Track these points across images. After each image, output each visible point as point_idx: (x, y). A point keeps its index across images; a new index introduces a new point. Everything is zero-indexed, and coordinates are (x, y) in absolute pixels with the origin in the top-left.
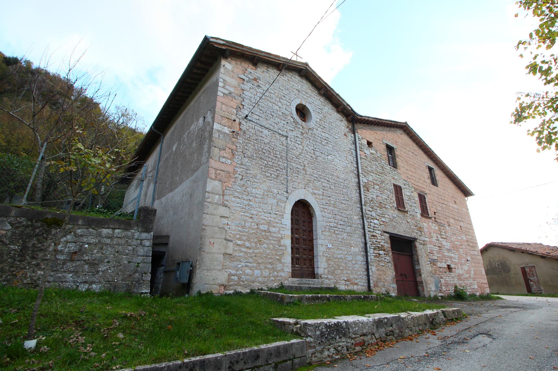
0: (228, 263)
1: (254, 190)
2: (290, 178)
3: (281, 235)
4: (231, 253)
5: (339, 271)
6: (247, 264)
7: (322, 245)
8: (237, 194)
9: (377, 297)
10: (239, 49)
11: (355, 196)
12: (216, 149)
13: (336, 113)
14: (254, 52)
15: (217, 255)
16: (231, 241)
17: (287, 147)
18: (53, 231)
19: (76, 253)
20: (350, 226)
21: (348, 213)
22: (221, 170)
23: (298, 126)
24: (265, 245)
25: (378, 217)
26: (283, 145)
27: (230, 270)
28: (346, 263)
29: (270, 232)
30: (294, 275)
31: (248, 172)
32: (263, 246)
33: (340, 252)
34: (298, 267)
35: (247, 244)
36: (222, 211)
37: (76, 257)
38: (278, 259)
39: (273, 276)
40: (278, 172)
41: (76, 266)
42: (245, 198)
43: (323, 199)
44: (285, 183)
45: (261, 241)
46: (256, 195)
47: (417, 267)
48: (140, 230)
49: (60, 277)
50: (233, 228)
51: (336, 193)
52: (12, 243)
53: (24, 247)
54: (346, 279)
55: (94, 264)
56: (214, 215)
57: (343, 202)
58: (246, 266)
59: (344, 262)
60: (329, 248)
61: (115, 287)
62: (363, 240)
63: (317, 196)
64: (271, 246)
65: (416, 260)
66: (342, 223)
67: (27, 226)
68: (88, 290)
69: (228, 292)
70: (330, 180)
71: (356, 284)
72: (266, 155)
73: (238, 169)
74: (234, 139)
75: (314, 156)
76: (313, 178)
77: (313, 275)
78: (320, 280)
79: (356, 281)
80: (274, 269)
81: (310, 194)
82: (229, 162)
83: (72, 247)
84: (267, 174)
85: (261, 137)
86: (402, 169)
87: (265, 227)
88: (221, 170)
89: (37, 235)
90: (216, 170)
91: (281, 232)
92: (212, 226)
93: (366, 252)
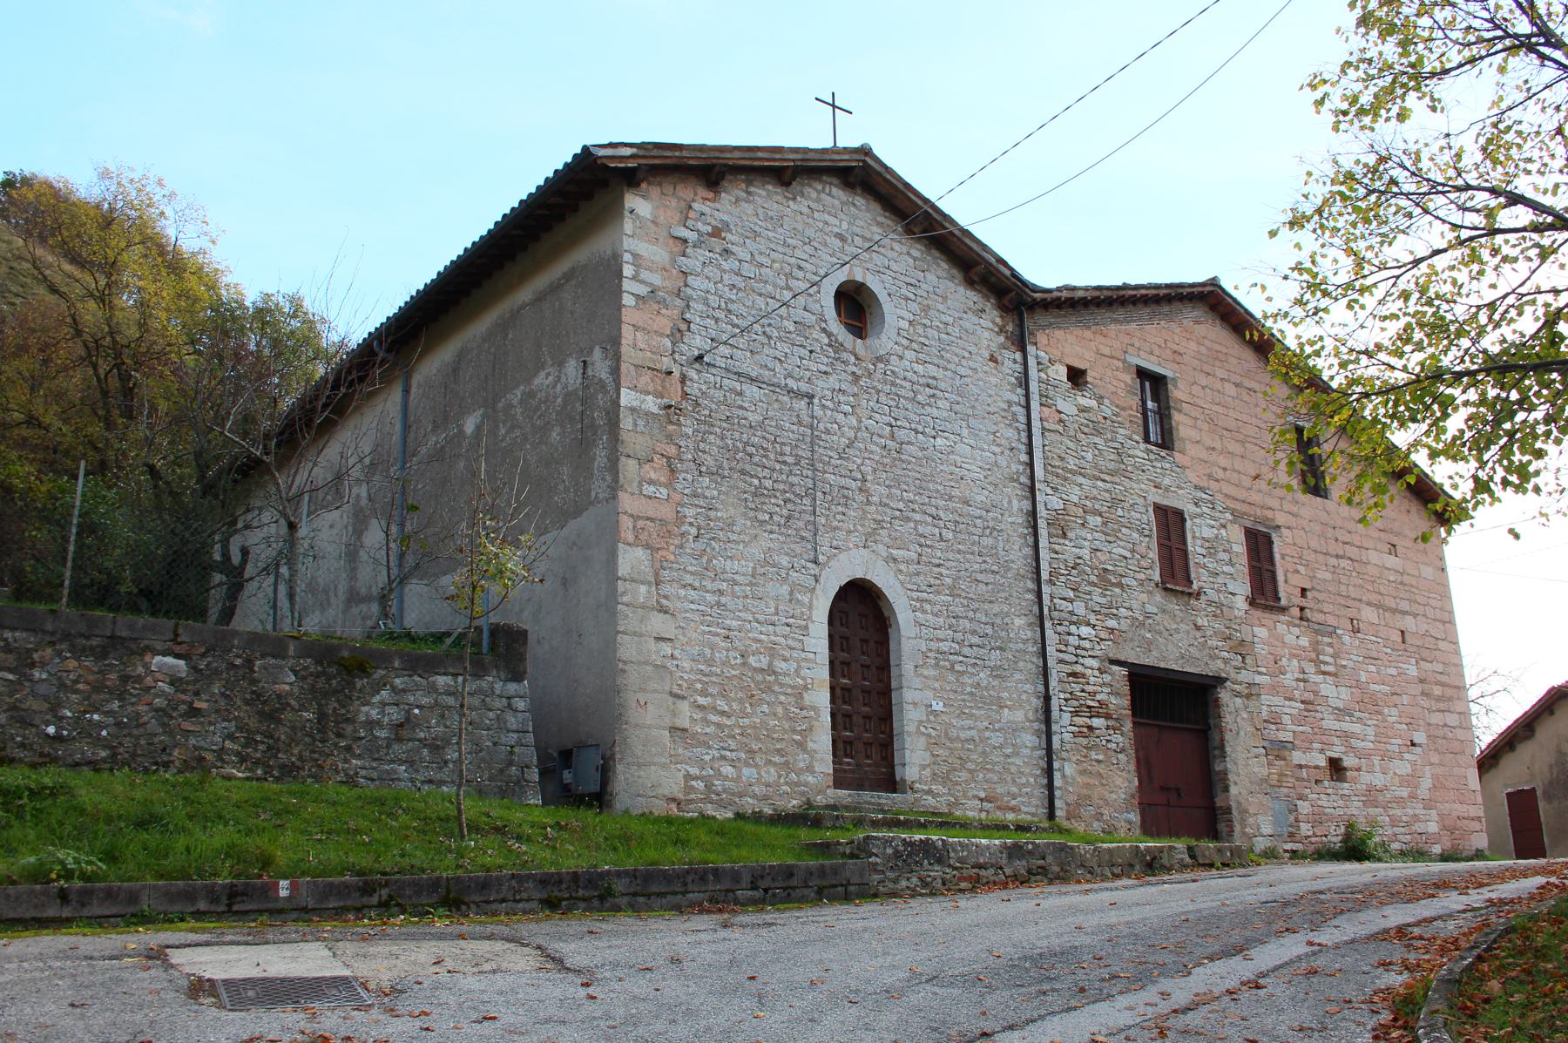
0: (680, 751)
1: (729, 562)
3: (804, 679)
5: (964, 775)
8: (689, 579)
11: (1018, 554)
13: (961, 289)
14: (713, 154)
15: (655, 732)
16: (684, 698)
19: (401, 725)
20: (1001, 649)
21: (996, 608)
23: (845, 356)
24: (765, 707)
26: (800, 423)
28: (984, 752)
29: (774, 673)
30: (839, 783)
31: (712, 514)
32: (759, 710)
35: (722, 704)
36: (658, 623)
37: (404, 733)
39: (786, 783)
40: (789, 506)
43: (918, 574)
46: (737, 577)
47: (1218, 767)
51: (959, 552)
52: (303, 708)
53: (322, 716)
54: (983, 795)
55: (436, 747)
56: (641, 635)
57: (980, 577)
58: (723, 758)
59: (980, 749)
62: (1041, 688)
63: (902, 567)
64: (780, 710)
65: (1217, 743)
66: (975, 640)
67: (318, 675)
70: (941, 513)
71: (1013, 809)
72: (756, 459)
74: (671, 427)
75: (891, 444)
77: (891, 784)
78: (910, 797)
79: (1013, 803)
81: (881, 563)
82: (664, 491)
83: (395, 714)
85: (741, 407)
86: (1192, 450)
87: (764, 662)
89: (336, 692)
90: (636, 518)
91: (804, 672)
92: (639, 663)
93: (1048, 721)
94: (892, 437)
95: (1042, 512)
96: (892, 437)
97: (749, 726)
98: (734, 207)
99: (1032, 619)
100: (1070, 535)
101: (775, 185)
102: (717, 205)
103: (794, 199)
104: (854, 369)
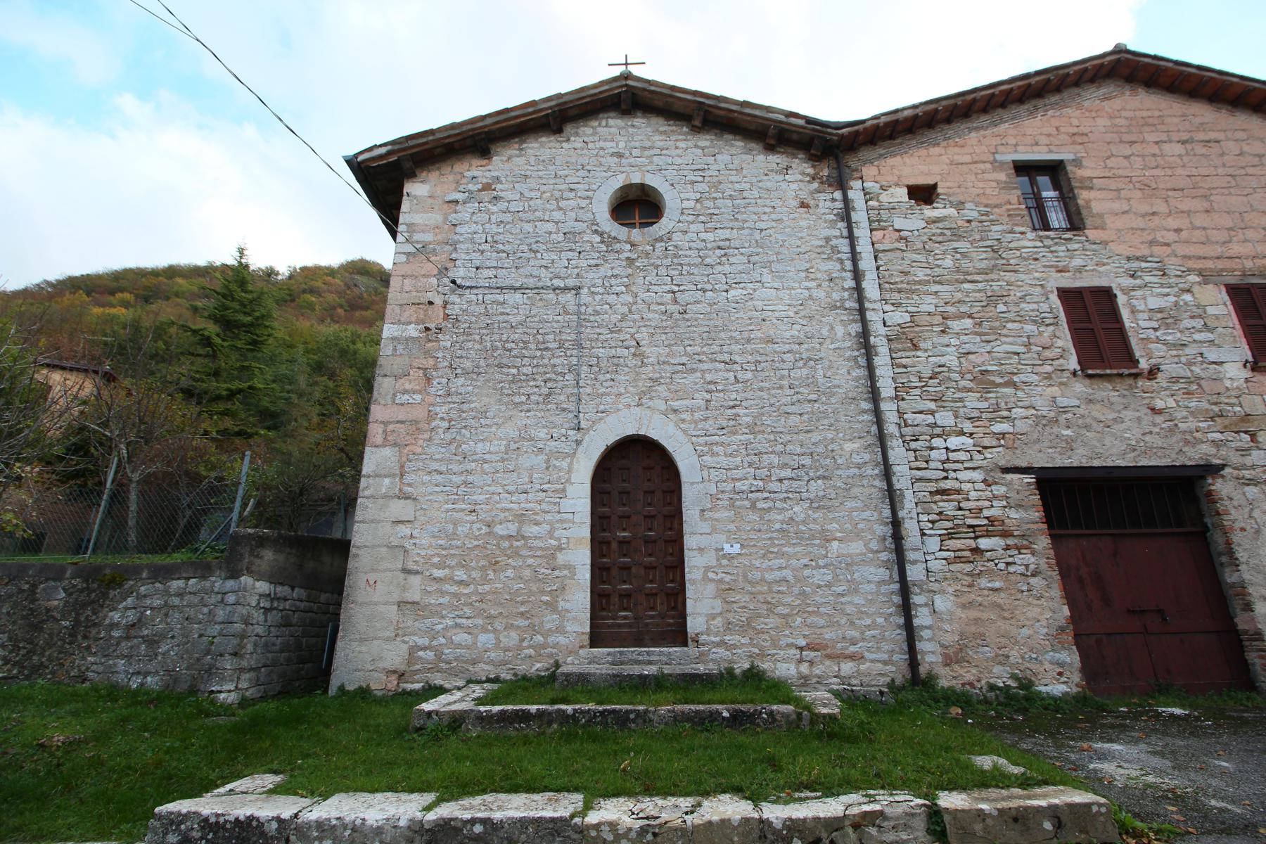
0: (410, 623)
1: (480, 445)
2: (589, 390)
3: (559, 539)
4: (417, 598)
5: (772, 621)
6: (458, 621)
7: (700, 550)
8: (435, 466)
9: (799, 715)
11: (847, 377)
12: (387, 380)
13: (761, 157)
14: (465, 128)
15: (382, 608)
16: (417, 572)
17: (579, 313)
18: (112, 593)
19: (134, 625)
20: (824, 478)
21: (815, 437)
22: (398, 422)
23: (617, 246)
24: (510, 573)
25: (968, 427)
26: (566, 313)
27: (415, 638)
28: (803, 593)
29: (523, 537)
31: (465, 407)
33: (782, 562)
34: (625, 618)
35: (460, 574)
36: (399, 509)
37: (133, 633)
38: (546, 603)
39: (530, 647)
40: (549, 385)
41: (132, 647)
42: (455, 467)
43: (706, 420)
44: (572, 406)
45: (497, 562)
46: (486, 456)
47: (1230, 578)
48: (223, 575)
49: (110, 666)
50: (424, 543)
51: (761, 389)
52: (64, 618)
53: (77, 622)
54: (803, 643)
55: (152, 642)
56: (379, 521)
58: (457, 625)
59: (796, 590)
60: (730, 557)
61: (175, 681)
62: (887, 513)
63: (684, 416)
64: (527, 573)
65: (1222, 547)
66: (788, 473)
67: (82, 591)
68: (142, 684)
69: (409, 687)
70: (736, 358)
71: (851, 657)
72: (514, 352)
73: (438, 409)
74: (430, 345)
75: (673, 308)
76: (669, 368)
77: (679, 635)
78: (691, 650)
79: (852, 649)
80: (534, 629)
81: (657, 417)
82: (418, 397)
83: (131, 616)
84: (517, 399)
85: (502, 314)
86: (1113, 223)
87: (512, 528)
88: (398, 422)
89: (93, 602)
90: (385, 423)
91: (557, 534)
92: (373, 547)
93: (899, 550)
94: (676, 302)
95: (877, 328)
96: (676, 302)
97: (488, 593)
98: (507, 164)
99: (871, 440)
100: (922, 345)
101: (548, 136)
102: (490, 167)
103: (568, 140)
104: (629, 255)
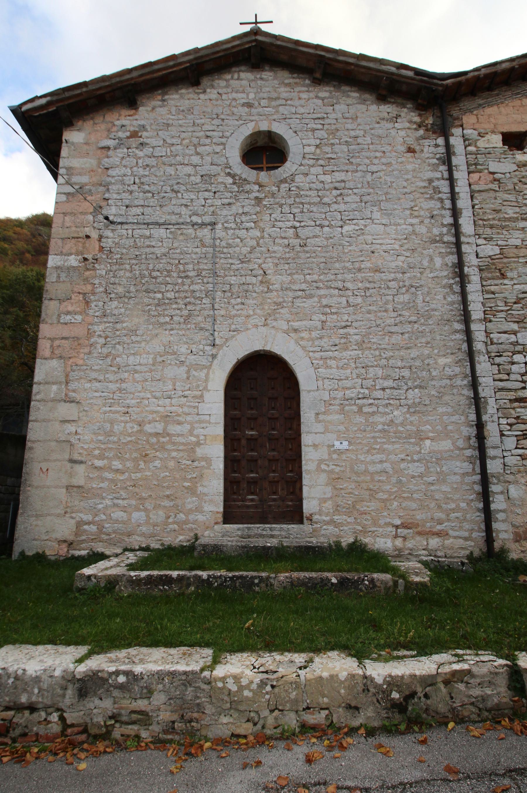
0: (77, 503)
1: (131, 358)
2: (222, 312)
3: (197, 436)
4: (82, 482)
5: (373, 505)
6: (116, 501)
7: (315, 446)
8: (94, 375)
9: (396, 583)
10: (81, 94)
11: (443, 302)
12: (52, 303)
13: (374, 107)
14: (114, 81)
16: (81, 462)
17: (214, 246)
20: (420, 387)
21: (414, 353)
22: (63, 338)
23: (247, 187)
24: (157, 463)
27: (81, 515)
29: (168, 435)
30: (228, 517)
31: (118, 326)
32: (151, 465)
33: (383, 457)
34: (252, 500)
35: (117, 464)
36: (64, 410)
38: (186, 488)
39: (174, 523)
40: (189, 307)
42: (111, 377)
45: (146, 455)
46: (136, 367)
54: (398, 522)
56: (49, 421)
57: (393, 329)
58: (115, 505)
59: (394, 480)
60: (340, 452)
62: (473, 417)
63: (303, 335)
64: (172, 464)
69: (77, 553)
70: (349, 285)
71: (438, 534)
72: (159, 280)
73: (96, 328)
74: (87, 273)
76: (291, 294)
77: (295, 514)
78: (306, 527)
79: (439, 527)
81: (280, 335)
82: (79, 318)
84: (162, 320)
85: (149, 246)
87: (159, 427)
88: (63, 338)
90: (52, 340)
91: (195, 432)
93: (482, 448)
94: (297, 236)
95: (470, 259)
96: (297, 236)
97: (140, 479)
98: (154, 114)
99: (461, 356)
100: (509, 274)
101: (187, 88)
102: (136, 117)
103: (204, 92)
104: (257, 194)
